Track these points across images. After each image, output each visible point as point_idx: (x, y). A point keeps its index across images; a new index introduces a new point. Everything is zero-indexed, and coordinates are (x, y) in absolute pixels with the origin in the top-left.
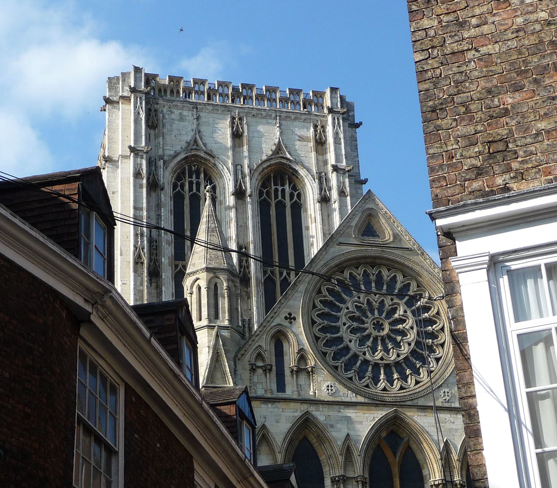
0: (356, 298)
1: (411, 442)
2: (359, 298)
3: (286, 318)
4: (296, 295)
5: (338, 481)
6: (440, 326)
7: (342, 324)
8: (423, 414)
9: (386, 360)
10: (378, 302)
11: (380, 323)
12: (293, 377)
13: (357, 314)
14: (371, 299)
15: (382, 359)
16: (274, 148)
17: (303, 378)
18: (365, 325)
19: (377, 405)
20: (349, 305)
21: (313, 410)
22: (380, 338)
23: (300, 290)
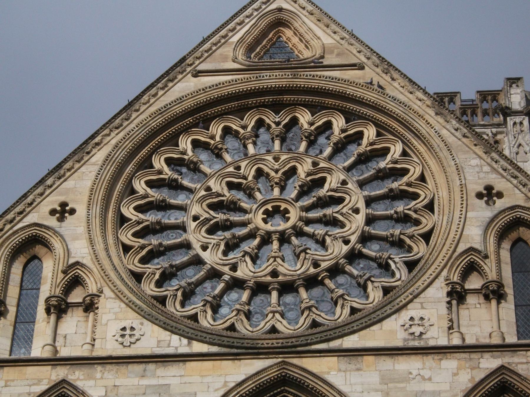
2: (238, 168)
4: (83, 169)
8: (352, 366)
9: (285, 275)
14: (266, 169)
15: (274, 274)
19: (235, 357)
20: (213, 184)
21: (78, 379)
22: (274, 237)
23: (93, 160)
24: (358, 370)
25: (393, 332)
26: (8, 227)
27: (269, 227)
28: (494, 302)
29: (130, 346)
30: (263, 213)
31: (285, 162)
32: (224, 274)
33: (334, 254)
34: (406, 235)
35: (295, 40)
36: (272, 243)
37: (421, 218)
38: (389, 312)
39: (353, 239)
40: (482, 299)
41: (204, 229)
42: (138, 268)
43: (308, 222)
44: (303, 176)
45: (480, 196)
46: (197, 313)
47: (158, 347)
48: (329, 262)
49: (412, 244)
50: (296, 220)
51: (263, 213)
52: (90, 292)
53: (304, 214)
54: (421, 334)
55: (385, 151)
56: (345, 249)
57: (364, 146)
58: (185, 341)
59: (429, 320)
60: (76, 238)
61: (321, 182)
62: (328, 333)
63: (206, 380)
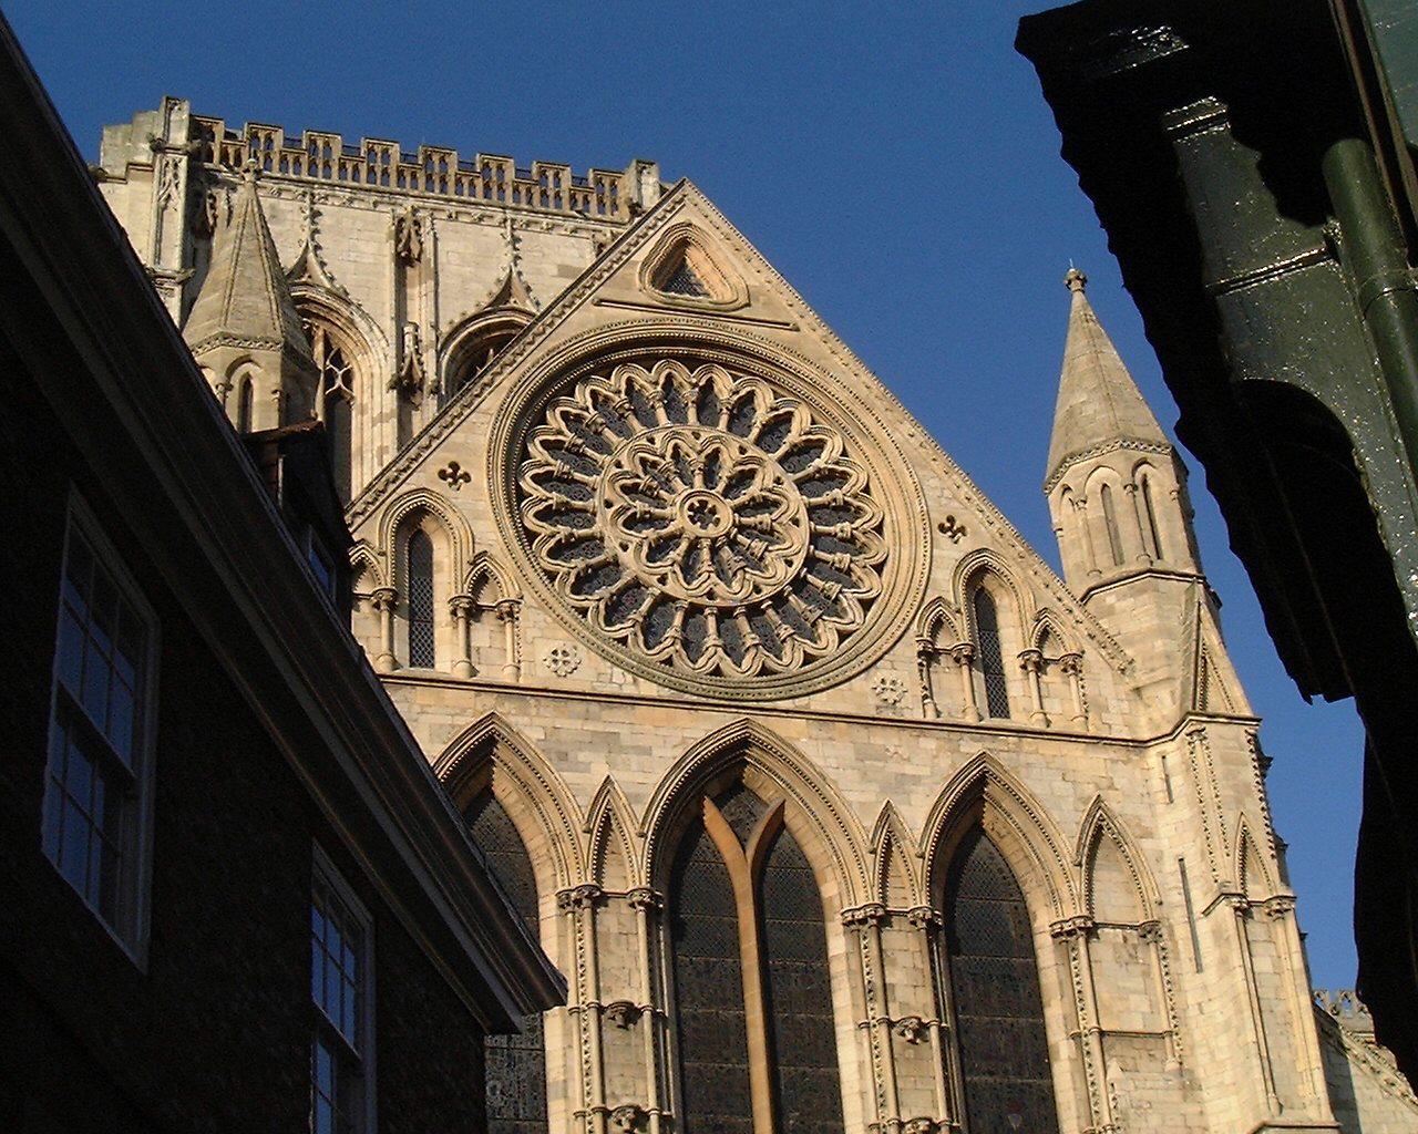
0: (644, 442)
1: (789, 814)
2: (652, 441)
3: (443, 475)
5: (578, 902)
6: (875, 522)
7: (620, 550)
8: (823, 734)
9: (724, 599)
10: (703, 455)
11: (710, 506)
12: (456, 628)
13: (644, 481)
15: (711, 595)
16: (496, 290)
17: (483, 632)
18: (667, 512)
21: (509, 713)
24: (830, 738)
25: (863, 695)
26: (392, 487)
27: (695, 530)
28: (965, 669)
35: (706, 267)
36: (701, 549)
40: (951, 663)
41: (621, 520)
43: (742, 528)
44: (729, 464)
45: (942, 528)
46: (627, 636)
49: (863, 576)
50: (730, 525)
55: (820, 444)
56: (792, 571)
57: (794, 436)
58: (629, 677)
60: (478, 516)
61: (751, 474)
63: (663, 732)
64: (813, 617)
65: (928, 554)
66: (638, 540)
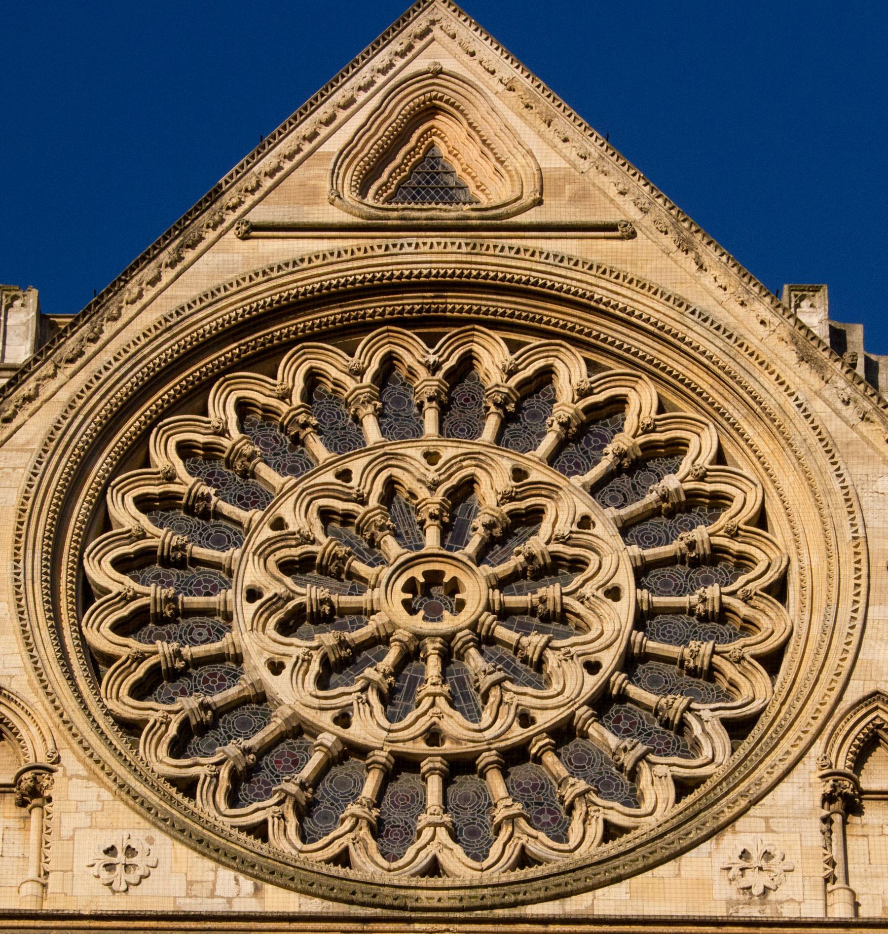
6: (772, 576)
10: (442, 489)
22: (432, 647)
25: (703, 884)
29: (127, 890)
30: (405, 589)
31: (452, 466)
32: (322, 730)
33: (567, 693)
34: (727, 655)
37: (758, 615)
38: (693, 836)
39: (609, 659)
42: (129, 708)
44: (491, 500)
46: (265, 822)
47: (188, 896)
48: (555, 713)
50: (480, 609)
51: (405, 589)
52: (32, 761)
53: (496, 595)
54: (766, 890)
56: (592, 683)
58: (247, 885)
59: (783, 859)
61: (534, 516)
62: (562, 879)
64: (628, 760)
65: (860, 616)
66: (300, 652)
